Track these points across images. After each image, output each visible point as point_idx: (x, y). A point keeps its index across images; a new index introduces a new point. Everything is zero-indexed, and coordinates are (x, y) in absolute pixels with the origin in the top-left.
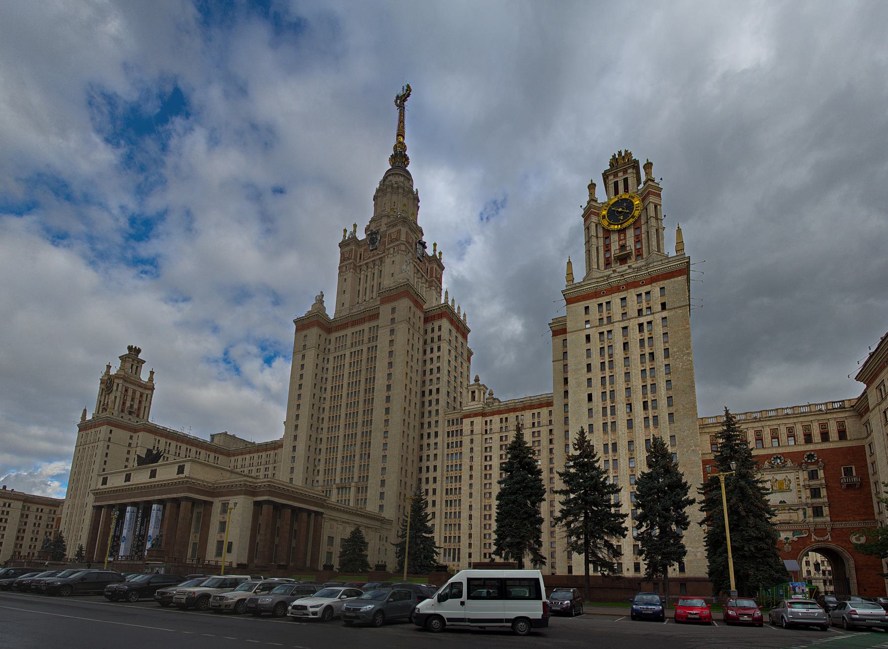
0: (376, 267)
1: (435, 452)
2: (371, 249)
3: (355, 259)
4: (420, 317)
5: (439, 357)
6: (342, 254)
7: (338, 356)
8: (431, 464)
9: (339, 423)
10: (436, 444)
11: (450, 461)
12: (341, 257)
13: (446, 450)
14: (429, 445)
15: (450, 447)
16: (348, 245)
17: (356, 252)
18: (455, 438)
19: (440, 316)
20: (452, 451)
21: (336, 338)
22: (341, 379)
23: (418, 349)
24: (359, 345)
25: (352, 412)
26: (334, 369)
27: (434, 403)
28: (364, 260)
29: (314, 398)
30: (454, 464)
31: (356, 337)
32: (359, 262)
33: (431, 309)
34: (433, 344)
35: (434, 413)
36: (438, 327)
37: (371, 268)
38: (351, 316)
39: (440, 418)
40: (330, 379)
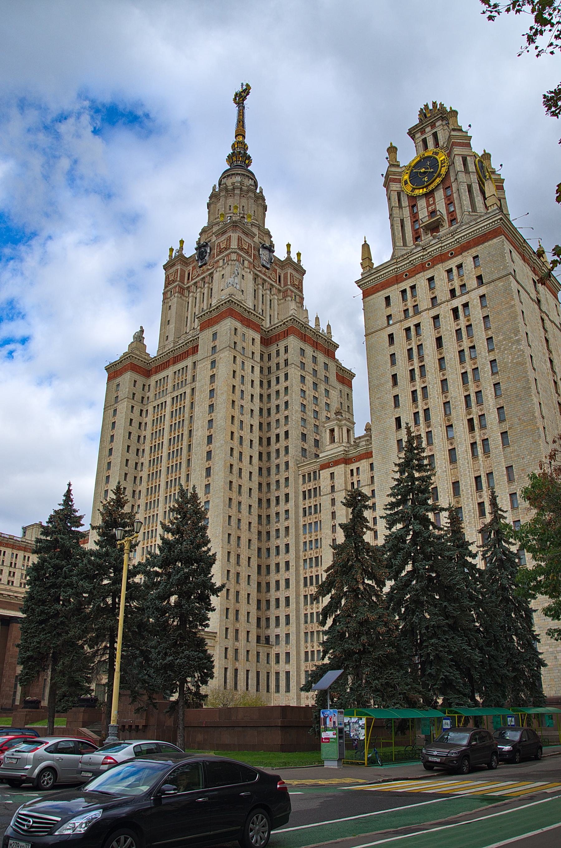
0: (206, 285)
1: (286, 524)
2: (200, 264)
3: (182, 280)
4: (253, 339)
5: (286, 388)
6: (167, 278)
7: (158, 405)
8: (281, 542)
9: (159, 496)
10: (287, 511)
11: (308, 536)
12: (166, 280)
13: (301, 519)
14: (278, 514)
15: (307, 514)
16: (174, 265)
17: (183, 271)
18: (312, 499)
19: (286, 334)
20: (310, 519)
21: (157, 382)
22: (161, 434)
23: (252, 381)
24: (182, 387)
25: (173, 478)
26: (153, 423)
27: (282, 452)
28: (192, 280)
29: (127, 465)
30: (313, 539)
31: (179, 377)
32: (188, 283)
33: (274, 327)
34: (279, 372)
35: (282, 467)
36: (284, 349)
37: (201, 287)
38: (172, 351)
39: (291, 474)
40: (148, 437)
